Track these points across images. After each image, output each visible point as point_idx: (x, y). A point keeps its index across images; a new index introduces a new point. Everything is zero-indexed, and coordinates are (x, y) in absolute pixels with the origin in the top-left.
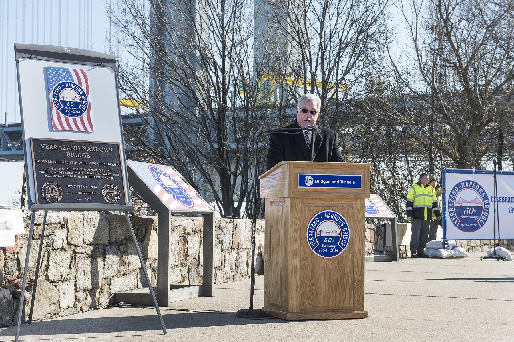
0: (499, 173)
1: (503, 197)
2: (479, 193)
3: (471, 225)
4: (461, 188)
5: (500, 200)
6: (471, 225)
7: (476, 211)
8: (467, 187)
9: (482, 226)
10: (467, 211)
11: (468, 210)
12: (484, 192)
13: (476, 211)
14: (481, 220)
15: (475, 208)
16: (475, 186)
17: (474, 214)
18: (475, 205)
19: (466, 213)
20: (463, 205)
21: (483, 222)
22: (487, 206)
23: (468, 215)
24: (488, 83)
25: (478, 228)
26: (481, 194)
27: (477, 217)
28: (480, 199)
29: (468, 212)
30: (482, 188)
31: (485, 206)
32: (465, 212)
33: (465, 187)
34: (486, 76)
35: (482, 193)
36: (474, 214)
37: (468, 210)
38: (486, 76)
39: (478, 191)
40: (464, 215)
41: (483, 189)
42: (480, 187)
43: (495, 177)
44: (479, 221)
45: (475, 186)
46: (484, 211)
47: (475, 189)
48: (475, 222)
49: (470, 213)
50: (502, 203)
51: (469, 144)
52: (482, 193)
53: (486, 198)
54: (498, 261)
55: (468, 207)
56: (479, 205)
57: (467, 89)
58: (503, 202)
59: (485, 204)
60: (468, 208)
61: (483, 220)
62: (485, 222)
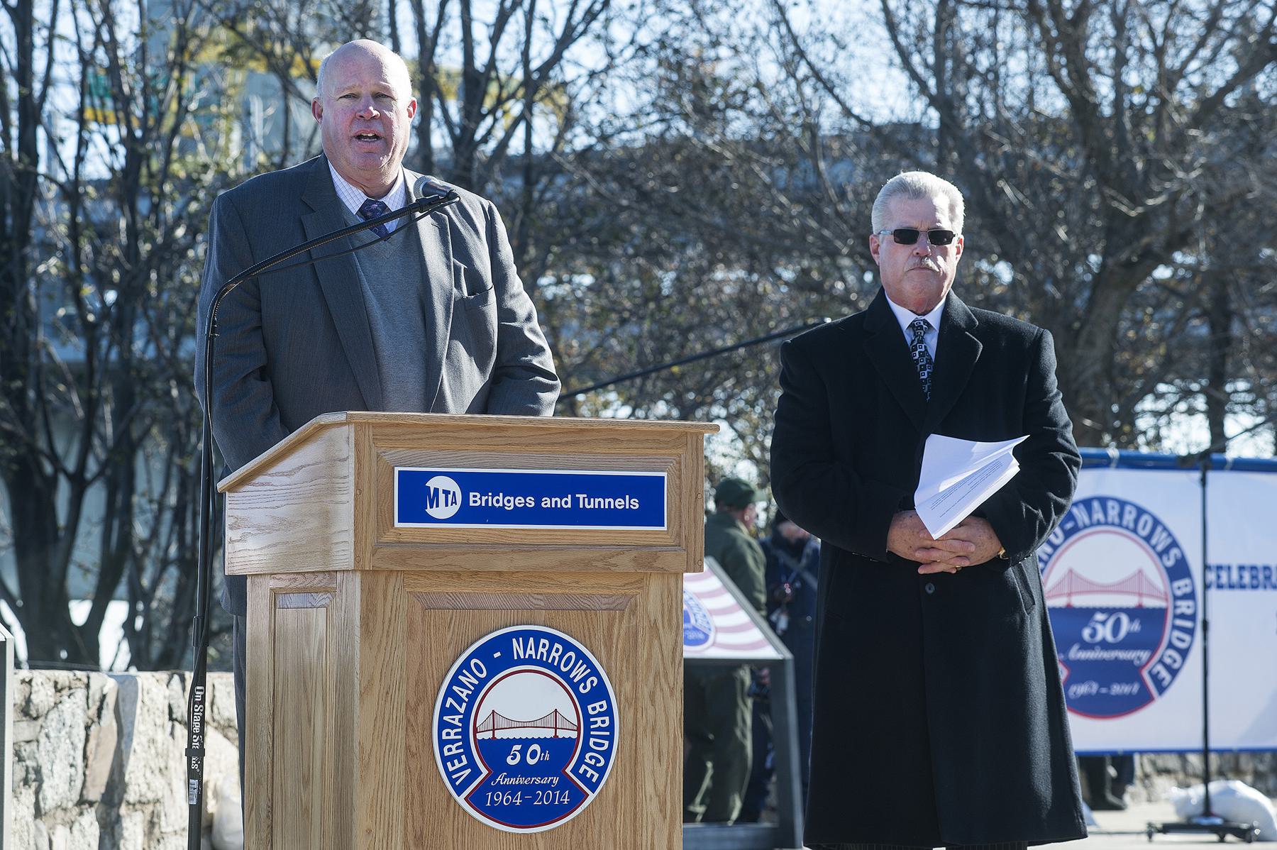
0: (1221, 466)
1: (1253, 568)
2: (1154, 547)
3: (1117, 689)
4: (1075, 530)
5: (1241, 577)
6: (1117, 689)
7: (1136, 627)
8: (1099, 523)
9: (1161, 689)
10: (1099, 627)
11: (1104, 623)
12: (1174, 544)
13: (1136, 627)
14: (1160, 668)
15: (1134, 613)
16: (1136, 521)
17: (1130, 643)
18: (1131, 601)
19: (1093, 635)
20: (1079, 601)
21: (1164, 674)
22: (1185, 608)
23: (1104, 645)
24: (1169, 79)
25: (1143, 699)
26: (1160, 555)
27: (1144, 655)
28: (1156, 576)
29: (1105, 633)
30: (1165, 529)
31: (1175, 607)
32: (1086, 633)
33: (1092, 525)
34: (1159, 53)
35: (1166, 551)
36: (1130, 643)
37: (1104, 623)
38: (1159, 53)
39: (1148, 539)
40: (1086, 646)
41: (1170, 535)
42: (1156, 522)
43: (1204, 482)
44: (1150, 672)
45: (1136, 521)
46: (1175, 627)
47: (1135, 531)
48: (1130, 672)
49: (1110, 638)
50: (1248, 593)
51: (1090, 343)
52: (1166, 551)
53: (1179, 570)
54: (1222, 840)
55: (1102, 610)
56: (1150, 603)
57: (1081, 101)
58: (1254, 587)
59: (1176, 598)
60: (1100, 617)
61: (1168, 668)
62: (1174, 673)
